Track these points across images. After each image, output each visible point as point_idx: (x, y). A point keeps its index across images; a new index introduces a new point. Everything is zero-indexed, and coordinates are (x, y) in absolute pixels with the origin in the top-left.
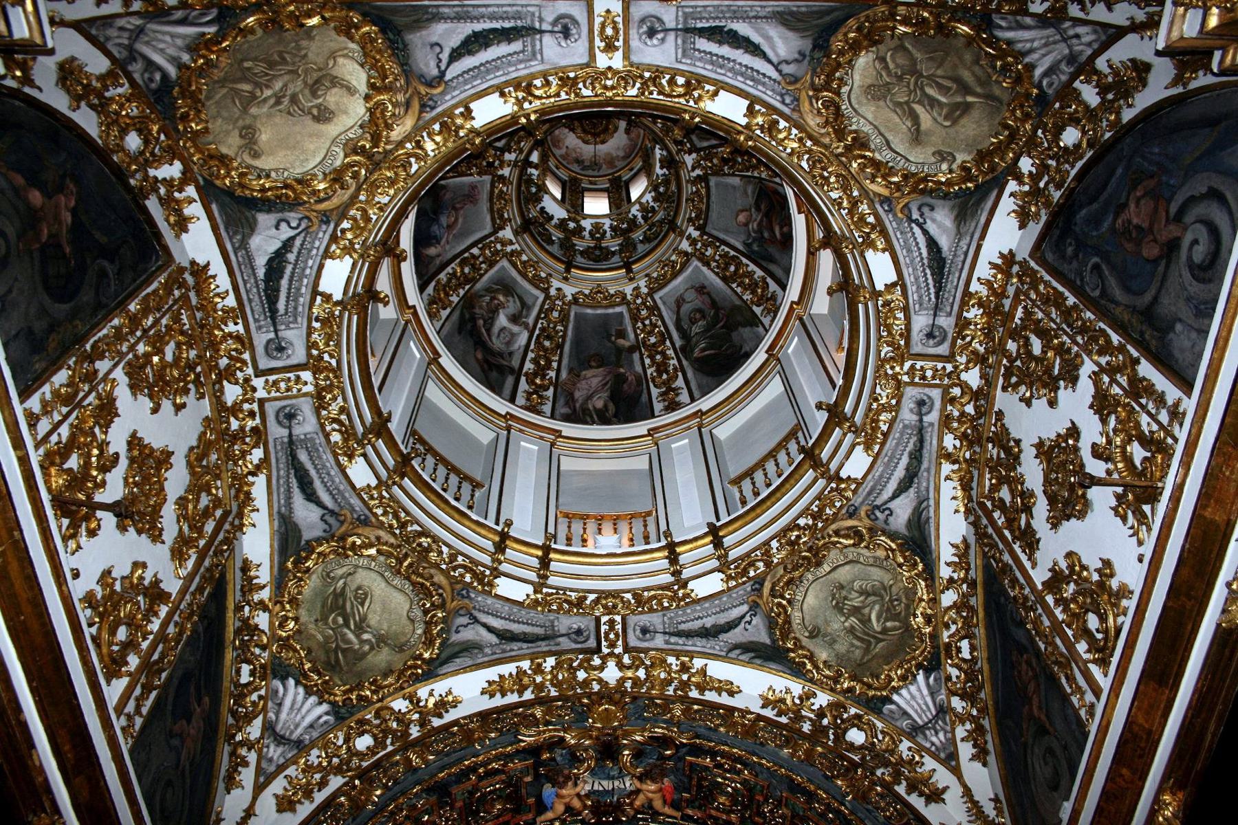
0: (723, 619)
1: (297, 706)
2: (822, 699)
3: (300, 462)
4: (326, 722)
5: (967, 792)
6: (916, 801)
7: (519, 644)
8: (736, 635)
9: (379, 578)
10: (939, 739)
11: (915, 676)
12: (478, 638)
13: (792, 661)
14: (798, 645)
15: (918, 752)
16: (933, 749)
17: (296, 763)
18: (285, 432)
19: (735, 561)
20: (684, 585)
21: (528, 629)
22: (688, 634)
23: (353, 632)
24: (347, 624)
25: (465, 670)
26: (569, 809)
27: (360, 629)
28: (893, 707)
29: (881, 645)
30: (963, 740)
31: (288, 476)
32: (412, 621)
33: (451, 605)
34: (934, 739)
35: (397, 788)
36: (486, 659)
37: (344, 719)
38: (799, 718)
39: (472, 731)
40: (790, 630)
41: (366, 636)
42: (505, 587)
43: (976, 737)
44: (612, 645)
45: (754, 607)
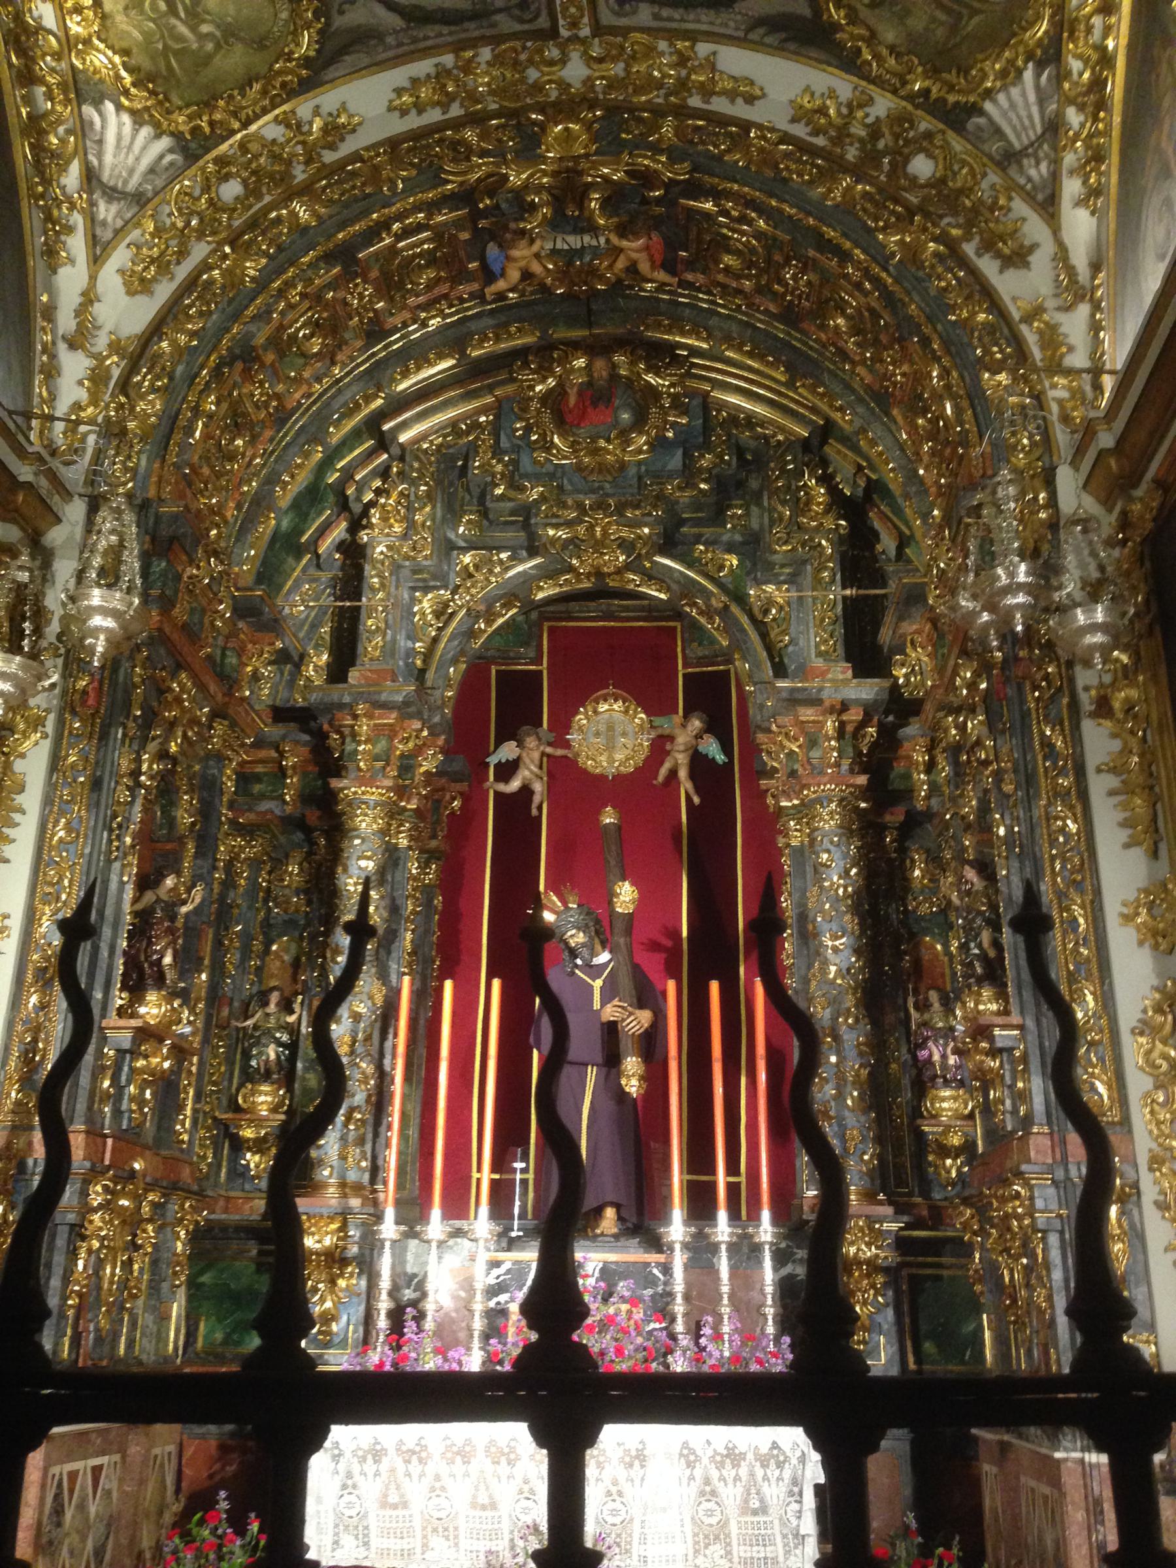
1: (126, 141)
2: (883, 105)
4: (172, 164)
6: (988, 266)
7: (437, 28)
10: (1038, 171)
13: (840, 46)
15: (1008, 189)
16: (1029, 186)
17: (138, 225)
25: (357, 72)
26: (527, 275)
28: (981, 121)
34: (1033, 172)
35: (282, 257)
36: (390, 54)
37: (197, 158)
38: (842, 135)
39: (376, 169)
44: (574, 25)
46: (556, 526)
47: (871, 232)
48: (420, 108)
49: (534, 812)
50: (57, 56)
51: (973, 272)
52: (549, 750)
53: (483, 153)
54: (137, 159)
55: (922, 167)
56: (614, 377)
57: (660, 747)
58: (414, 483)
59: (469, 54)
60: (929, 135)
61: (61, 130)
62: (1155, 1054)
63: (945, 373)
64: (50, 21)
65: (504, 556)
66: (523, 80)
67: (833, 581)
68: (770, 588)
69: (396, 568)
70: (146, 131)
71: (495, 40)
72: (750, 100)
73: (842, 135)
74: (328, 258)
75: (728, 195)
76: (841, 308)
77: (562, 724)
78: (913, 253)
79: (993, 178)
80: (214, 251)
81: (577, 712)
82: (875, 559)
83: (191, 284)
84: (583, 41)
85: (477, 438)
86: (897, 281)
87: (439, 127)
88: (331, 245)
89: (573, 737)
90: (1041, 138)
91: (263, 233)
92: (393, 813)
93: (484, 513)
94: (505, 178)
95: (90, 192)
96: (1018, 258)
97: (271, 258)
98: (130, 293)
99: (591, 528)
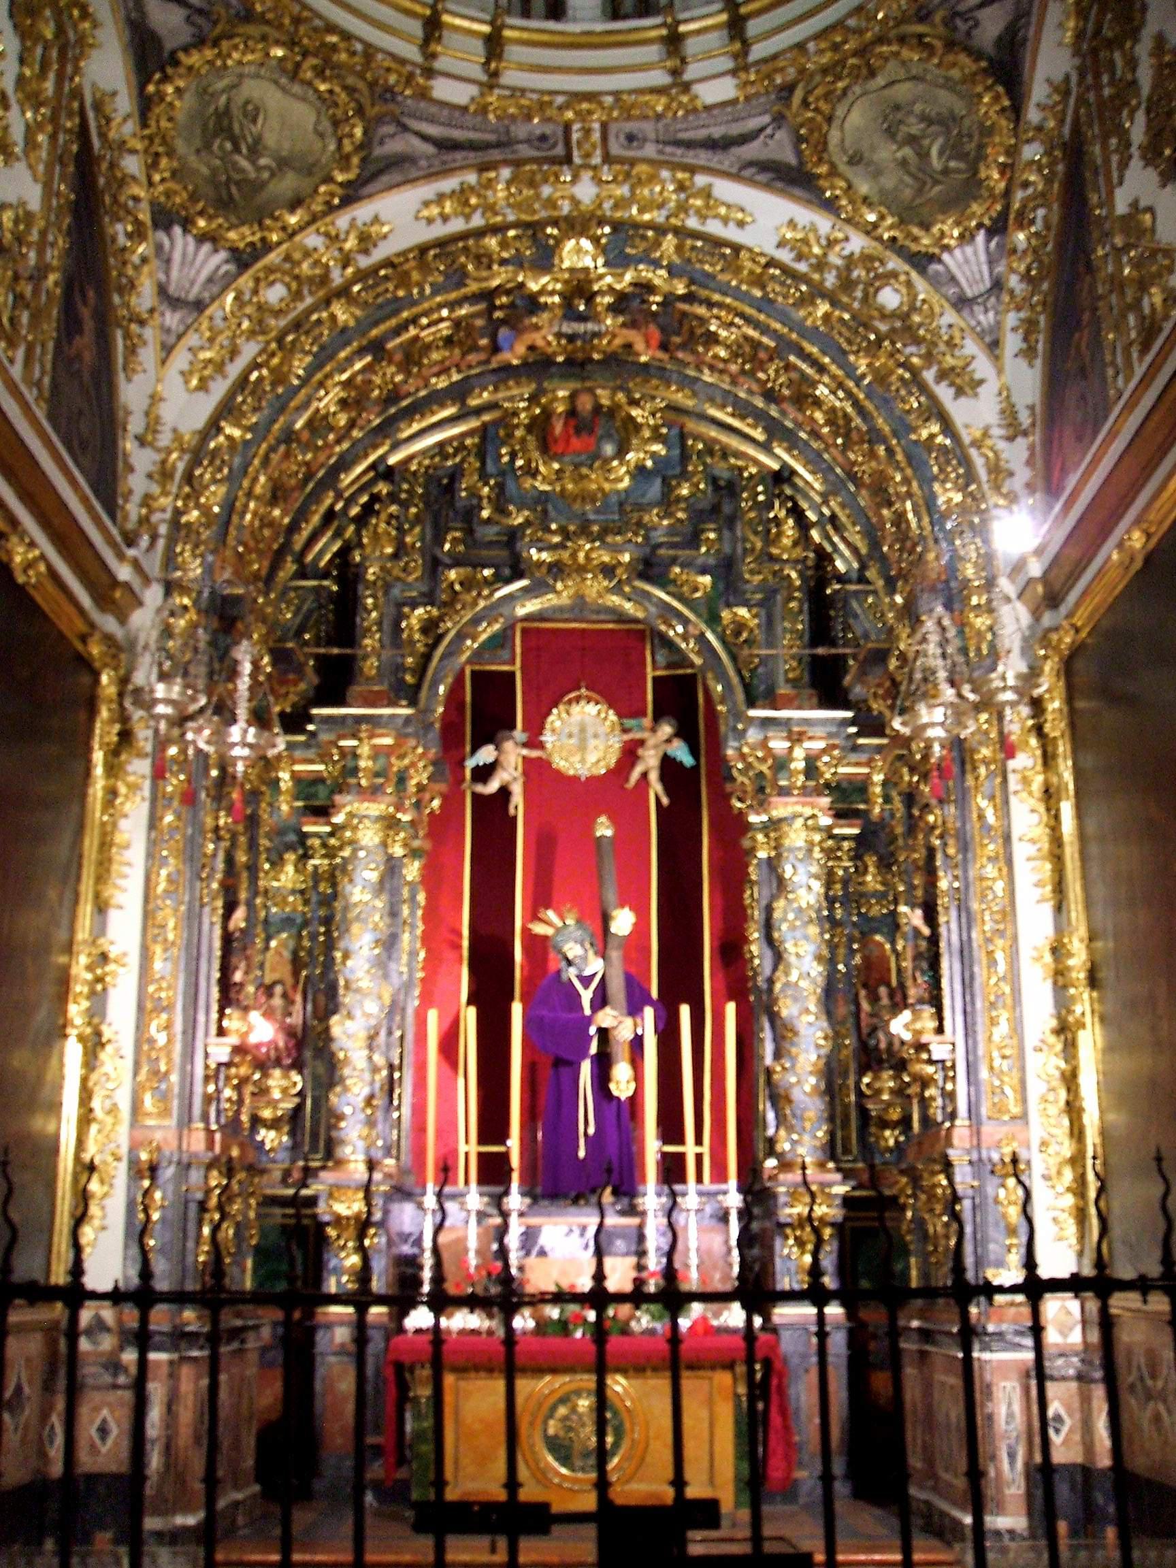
0: (736, 130)
2: (857, 243)
5: (1005, 394)
6: (944, 393)
7: (464, 154)
8: (751, 151)
9: (273, 87)
10: (987, 319)
11: (973, 237)
12: (409, 150)
14: (834, 172)
19: (757, 63)
20: (686, 87)
21: (472, 135)
22: (689, 145)
23: (247, 158)
24: (237, 149)
25: (390, 188)
27: (254, 152)
28: (939, 267)
29: (938, 188)
32: (321, 135)
33: (372, 112)
34: (982, 318)
38: (821, 265)
40: (825, 149)
41: (263, 161)
42: (443, 89)
43: (1029, 328)
44: (588, 155)
45: (779, 119)
46: (540, 550)
47: (845, 353)
48: (445, 218)
49: (512, 811)
51: (932, 397)
52: (525, 752)
53: (503, 262)
55: (889, 298)
57: (630, 754)
58: (405, 505)
59: (492, 174)
60: (894, 275)
63: (906, 481)
65: (487, 572)
67: (801, 611)
68: (743, 612)
70: (207, 247)
71: (517, 164)
73: (821, 265)
74: (361, 352)
75: (720, 305)
77: (536, 727)
80: (263, 351)
81: (549, 713)
83: (242, 382)
84: (595, 168)
85: (463, 461)
86: (868, 396)
87: (464, 236)
89: (548, 738)
91: (307, 333)
93: (469, 531)
97: (315, 355)
99: (574, 555)
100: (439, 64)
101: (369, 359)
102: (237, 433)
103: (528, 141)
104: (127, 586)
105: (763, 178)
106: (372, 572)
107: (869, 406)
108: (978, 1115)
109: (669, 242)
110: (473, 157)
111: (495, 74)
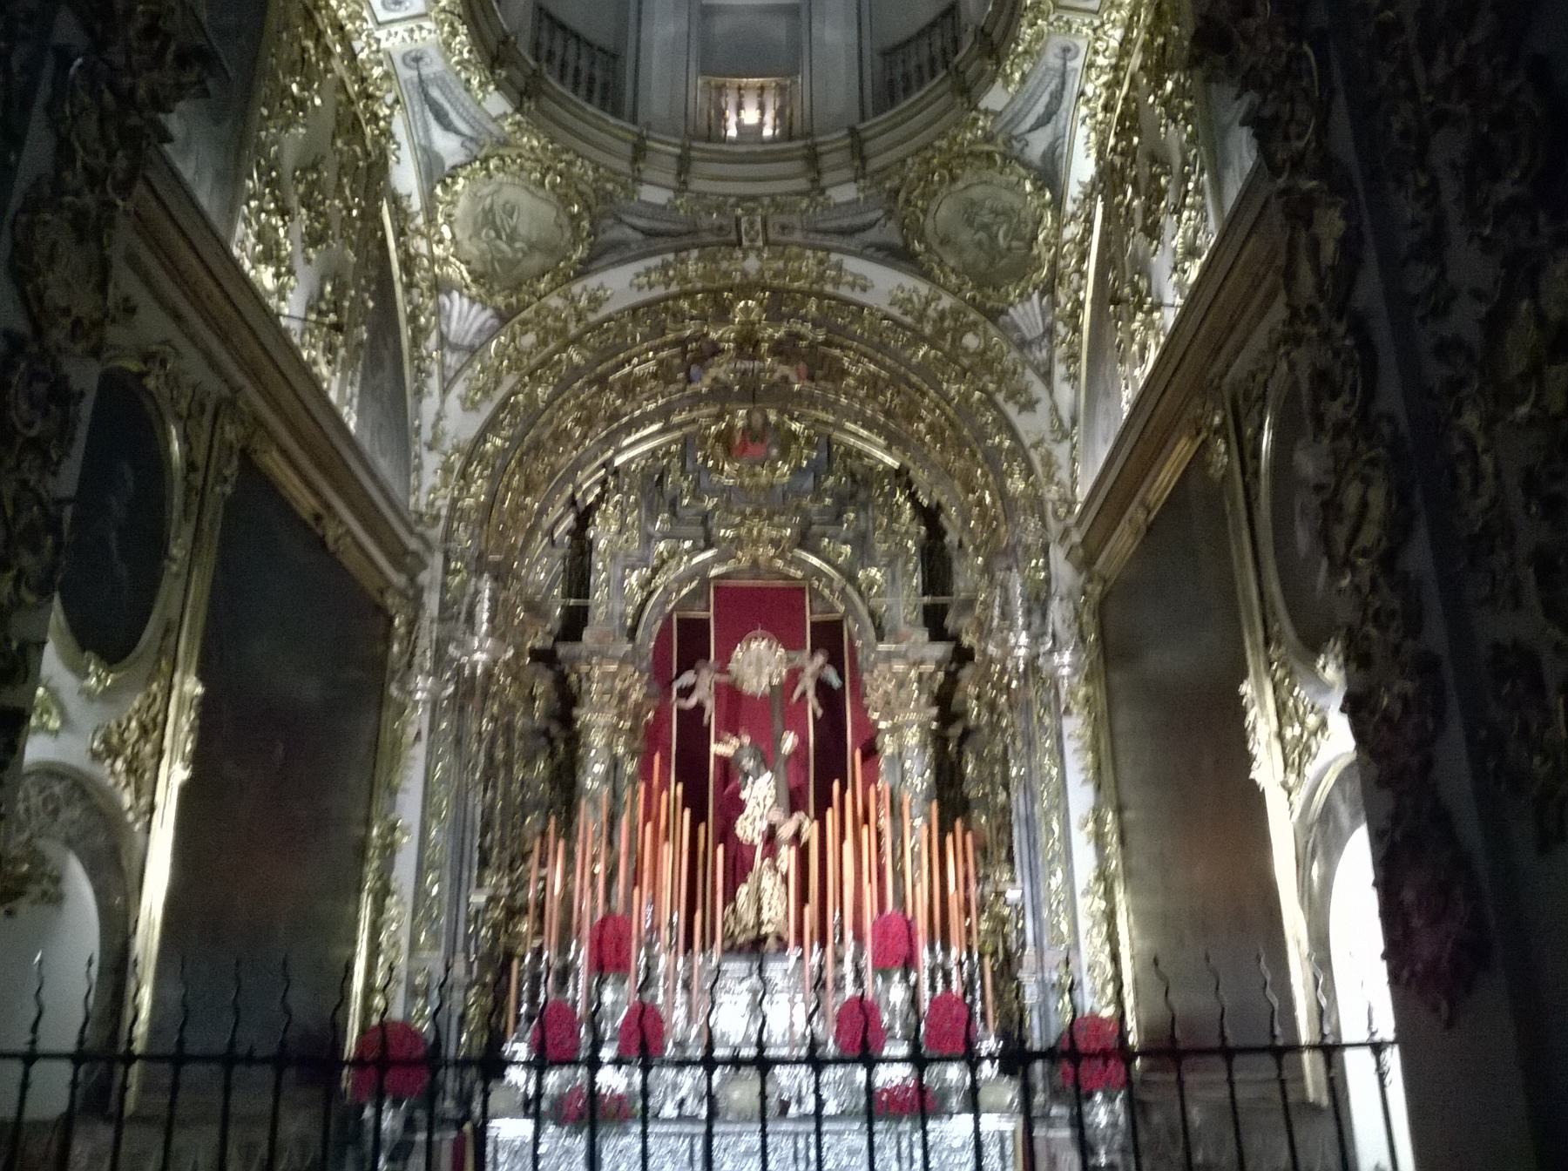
0: (858, 221)
1: (465, 314)
2: (947, 302)
3: (432, 98)
4: (492, 326)
6: (1011, 410)
7: (664, 239)
8: (872, 236)
11: (1030, 297)
14: (929, 249)
17: (471, 366)
18: (414, 73)
20: (822, 191)
22: (826, 232)
24: (499, 236)
25: (614, 264)
30: (1060, 361)
31: (423, 111)
32: (561, 227)
34: (1038, 354)
36: (632, 253)
37: (510, 320)
38: (921, 316)
41: (518, 245)
44: (752, 240)
45: (889, 214)
46: (726, 528)
48: (651, 286)
50: (427, 270)
51: (1001, 412)
52: (717, 677)
53: (692, 318)
54: (471, 325)
56: (766, 422)
57: (794, 675)
60: (975, 324)
61: (427, 313)
62: (1094, 908)
63: (984, 475)
64: (423, 248)
65: (688, 544)
66: (718, 270)
67: (915, 570)
69: (614, 556)
70: (477, 307)
71: (702, 247)
72: (864, 289)
74: (590, 383)
76: (921, 419)
77: (725, 656)
78: (966, 397)
79: (1014, 354)
82: (943, 547)
83: (504, 404)
87: (666, 298)
88: (593, 375)
89: (732, 666)
90: (1043, 335)
92: (614, 730)
93: (674, 514)
94: (707, 334)
95: (442, 349)
96: (1029, 406)
98: (465, 410)
99: (750, 531)
100: (644, 176)
101: (595, 388)
102: (498, 442)
103: (711, 230)
104: (415, 554)
105: (881, 255)
106: (602, 544)
107: (958, 421)
108: (1041, 943)
109: (812, 305)
110: (671, 242)
111: (685, 183)
